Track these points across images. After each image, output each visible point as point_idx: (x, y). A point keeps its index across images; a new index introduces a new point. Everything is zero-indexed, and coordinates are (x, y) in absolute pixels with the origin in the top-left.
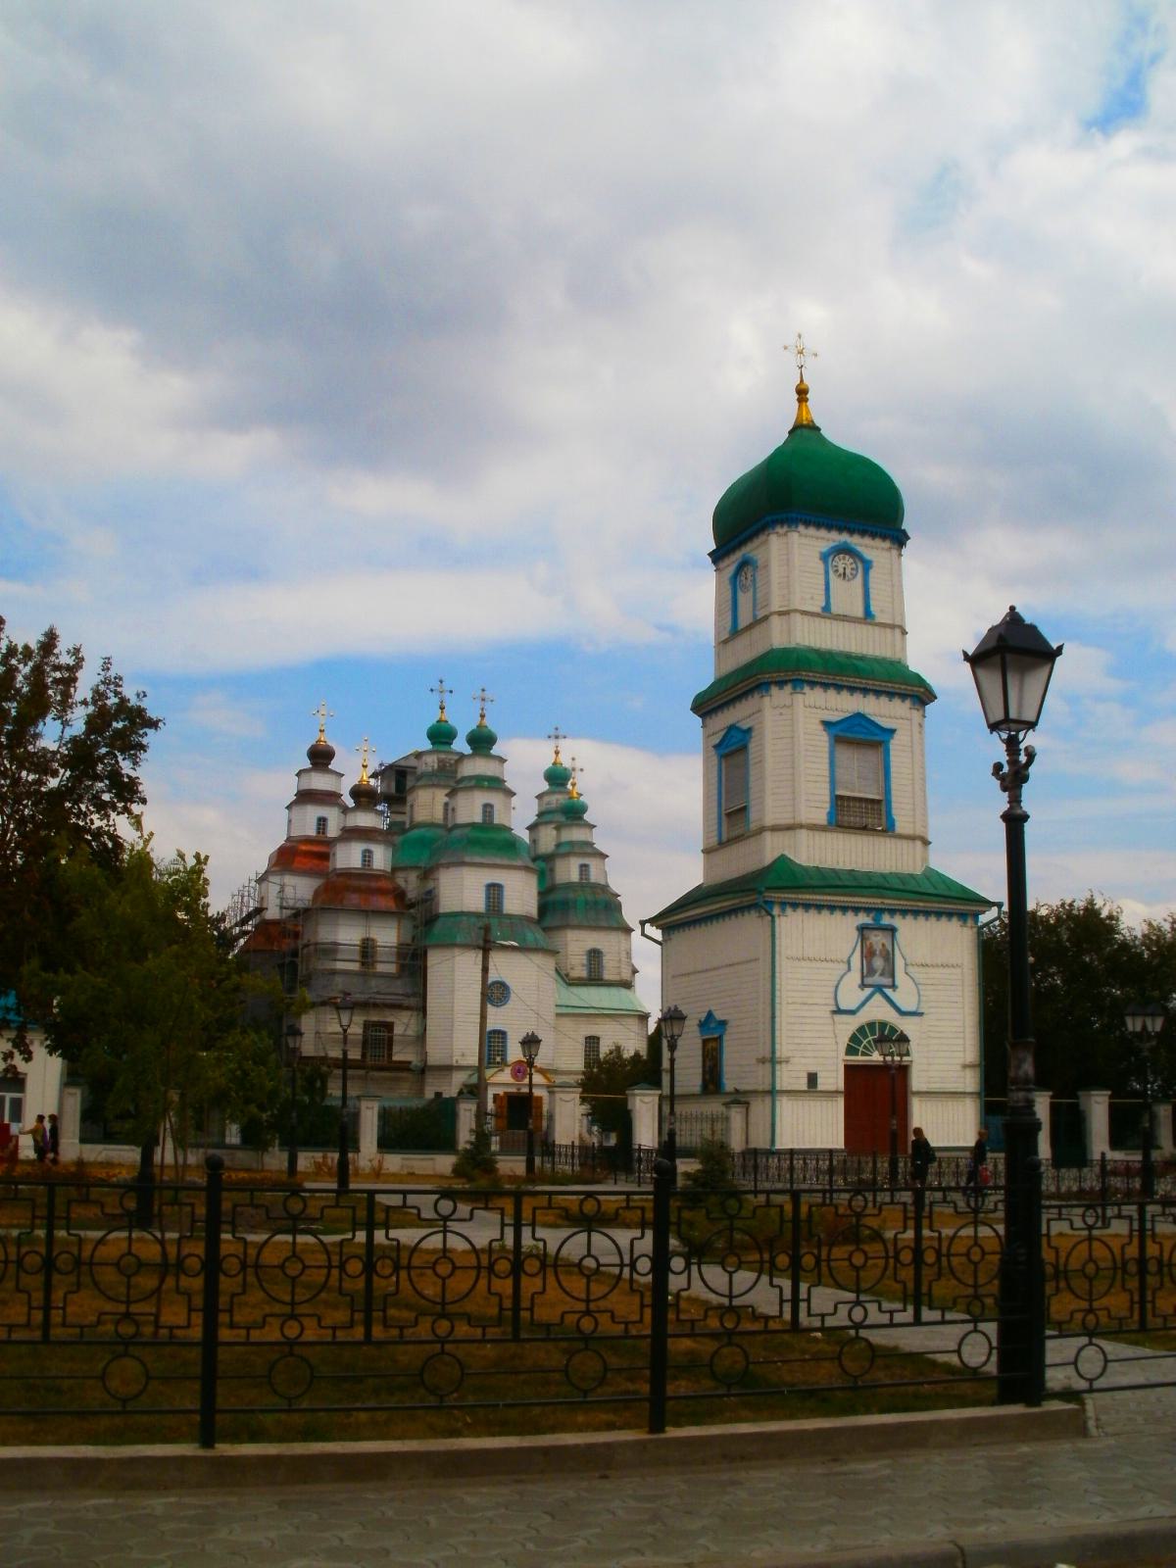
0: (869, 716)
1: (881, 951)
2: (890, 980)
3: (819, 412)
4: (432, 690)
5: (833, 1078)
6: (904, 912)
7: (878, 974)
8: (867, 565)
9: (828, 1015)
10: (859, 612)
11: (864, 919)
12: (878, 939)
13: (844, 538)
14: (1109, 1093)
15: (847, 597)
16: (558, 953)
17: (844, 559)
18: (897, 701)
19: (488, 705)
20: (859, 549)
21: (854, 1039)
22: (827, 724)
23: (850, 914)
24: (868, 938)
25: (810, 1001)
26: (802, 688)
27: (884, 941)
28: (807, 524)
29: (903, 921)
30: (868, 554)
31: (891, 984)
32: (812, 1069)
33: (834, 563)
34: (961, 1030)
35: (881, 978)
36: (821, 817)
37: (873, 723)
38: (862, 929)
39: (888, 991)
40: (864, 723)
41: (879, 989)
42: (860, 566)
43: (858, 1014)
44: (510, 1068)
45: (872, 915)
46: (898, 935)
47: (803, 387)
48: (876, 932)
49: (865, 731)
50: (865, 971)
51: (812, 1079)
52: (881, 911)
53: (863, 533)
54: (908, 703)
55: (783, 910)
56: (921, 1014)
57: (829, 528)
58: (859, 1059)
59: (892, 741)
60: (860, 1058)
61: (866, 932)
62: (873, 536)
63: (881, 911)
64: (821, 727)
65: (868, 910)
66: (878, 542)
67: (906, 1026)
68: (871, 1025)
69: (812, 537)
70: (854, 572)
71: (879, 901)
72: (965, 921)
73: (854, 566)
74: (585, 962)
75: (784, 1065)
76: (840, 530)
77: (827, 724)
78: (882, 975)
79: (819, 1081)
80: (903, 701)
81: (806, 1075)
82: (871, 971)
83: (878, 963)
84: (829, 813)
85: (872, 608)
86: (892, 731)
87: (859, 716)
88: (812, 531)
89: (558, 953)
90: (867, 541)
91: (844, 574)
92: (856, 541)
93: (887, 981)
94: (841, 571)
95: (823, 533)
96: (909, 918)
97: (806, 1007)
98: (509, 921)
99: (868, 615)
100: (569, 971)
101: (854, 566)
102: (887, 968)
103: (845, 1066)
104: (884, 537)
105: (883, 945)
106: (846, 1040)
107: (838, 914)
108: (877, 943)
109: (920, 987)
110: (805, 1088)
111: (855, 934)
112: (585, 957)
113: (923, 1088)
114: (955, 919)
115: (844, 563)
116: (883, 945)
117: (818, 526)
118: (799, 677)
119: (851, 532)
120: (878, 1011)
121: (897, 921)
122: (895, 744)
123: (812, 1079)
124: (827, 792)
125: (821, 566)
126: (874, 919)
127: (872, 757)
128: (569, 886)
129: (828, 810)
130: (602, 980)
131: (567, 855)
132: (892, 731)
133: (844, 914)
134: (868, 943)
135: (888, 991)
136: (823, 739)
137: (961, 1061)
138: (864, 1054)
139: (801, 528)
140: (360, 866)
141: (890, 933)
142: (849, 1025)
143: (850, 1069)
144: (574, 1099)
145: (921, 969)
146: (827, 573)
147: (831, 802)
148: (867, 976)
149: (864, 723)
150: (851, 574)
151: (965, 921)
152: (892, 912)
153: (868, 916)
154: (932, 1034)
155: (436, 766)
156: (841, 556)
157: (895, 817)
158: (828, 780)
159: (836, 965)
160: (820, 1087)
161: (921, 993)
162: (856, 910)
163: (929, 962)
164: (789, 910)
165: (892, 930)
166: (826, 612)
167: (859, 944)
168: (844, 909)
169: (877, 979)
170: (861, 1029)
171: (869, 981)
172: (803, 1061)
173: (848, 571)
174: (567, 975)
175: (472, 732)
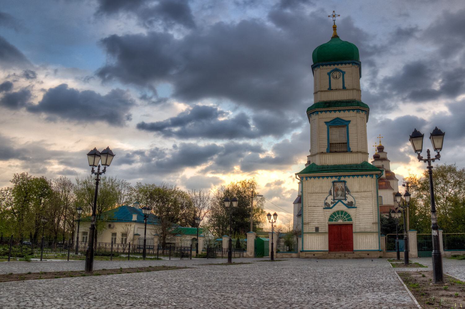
0: (342, 118)
1: (340, 189)
2: (345, 197)
3: (338, 33)
5: (325, 228)
6: (349, 176)
7: (339, 196)
8: (344, 73)
9: (323, 209)
10: (342, 88)
11: (334, 179)
12: (339, 185)
13: (336, 66)
14: (442, 231)
15: (337, 83)
17: (336, 73)
18: (351, 112)
20: (341, 69)
21: (331, 216)
22: (326, 123)
23: (330, 178)
24: (336, 185)
25: (316, 205)
26: (318, 113)
27: (342, 185)
28: (323, 65)
29: (349, 179)
30: (343, 70)
31: (345, 199)
32: (317, 226)
33: (333, 75)
34: (372, 212)
35: (341, 197)
36: (325, 150)
37: (342, 120)
38: (334, 182)
39: (344, 201)
40: (339, 120)
41: (340, 200)
42: (341, 73)
43: (333, 208)
45: (337, 178)
46: (347, 184)
47: (335, 26)
48: (339, 183)
49: (340, 122)
50: (335, 195)
51: (317, 229)
52: (341, 176)
53: (342, 64)
54: (355, 111)
55: (307, 179)
56: (356, 207)
57: (330, 65)
58: (333, 222)
59: (350, 124)
60: (334, 222)
61: (335, 183)
62: (345, 64)
63: (341, 176)
64: (325, 124)
65: (336, 177)
66: (347, 65)
67: (351, 212)
68: (338, 212)
69: (325, 69)
70: (340, 76)
71: (338, 173)
72: (372, 177)
73: (340, 74)
75: (307, 225)
76: (334, 64)
77: (326, 123)
78: (341, 196)
79: (320, 229)
80: (353, 111)
81: (315, 228)
82: (337, 195)
83: (340, 192)
84: (327, 149)
85: (346, 86)
86: (349, 121)
87: (338, 118)
88: (325, 67)
90: (344, 65)
91: (336, 77)
92: (339, 67)
93: (343, 198)
94: (335, 77)
95: (328, 67)
96: (351, 178)
97: (315, 207)
99: (344, 88)
101: (340, 74)
102: (343, 194)
103: (329, 225)
104: (349, 63)
105: (341, 187)
106: (329, 217)
107: (325, 179)
108: (339, 186)
109: (355, 199)
110: (315, 232)
111: (332, 184)
113: (358, 231)
114: (369, 177)
115: (337, 74)
116: (341, 187)
117: (326, 65)
118: (316, 110)
119: (338, 64)
120: (340, 207)
121: (347, 179)
122: (350, 125)
123: (317, 229)
124: (327, 143)
125: (328, 77)
126: (338, 179)
127: (344, 130)
129: (326, 148)
132: (349, 121)
133: (327, 179)
134: (336, 187)
135: (344, 201)
136: (326, 126)
137: (372, 222)
138: (335, 221)
139: (321, 67)
141: (344, 183)
142: (330, 212)
143: (330, 226)
144: (252, 236)
145: (356, 193)
146: (330, 78)
147: (328, 145)
148: (336, 197)
149: (339, 120)
150: (339, 77)
151: (372, 177)
152: (345, 176)
153: (336, 178)
154: (360, 214)
156: (335, 72)
157: (350, 147)
158: (327, 139)
159: (325, 194)
160: (320, 231)
161: (356, 201)
162: (332, 177)
163: (359, 191)
164: (309, 179)
165: (345, 182)
166: (330, 89)
167: (333, 188)
168: (327, 177)
169: (339, 197)
170: (334, 213)
171: (336, 198)
172: (313, 223)
173: (338, 76)
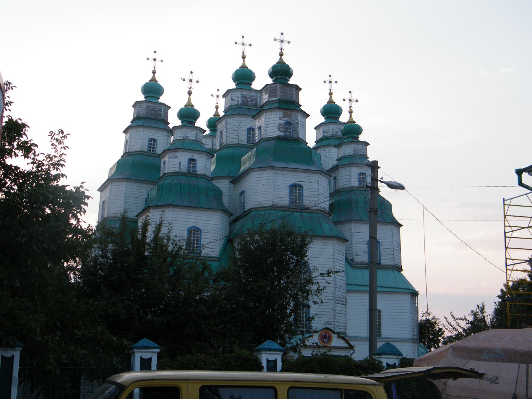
4: (236, 43)
16: (347, 241)
19: (285, 46)
44: (318, 335)
74: (366, 249)
89: (347, 241)
98: (308, 215)
100: (354, 256)
112: (366, 246)
128: (351, 190)
130: (379, 264)
131: (349, 165)
140: (186, 171)
155: (240, 101)
174: (352, 260)
175: (274, 67)
